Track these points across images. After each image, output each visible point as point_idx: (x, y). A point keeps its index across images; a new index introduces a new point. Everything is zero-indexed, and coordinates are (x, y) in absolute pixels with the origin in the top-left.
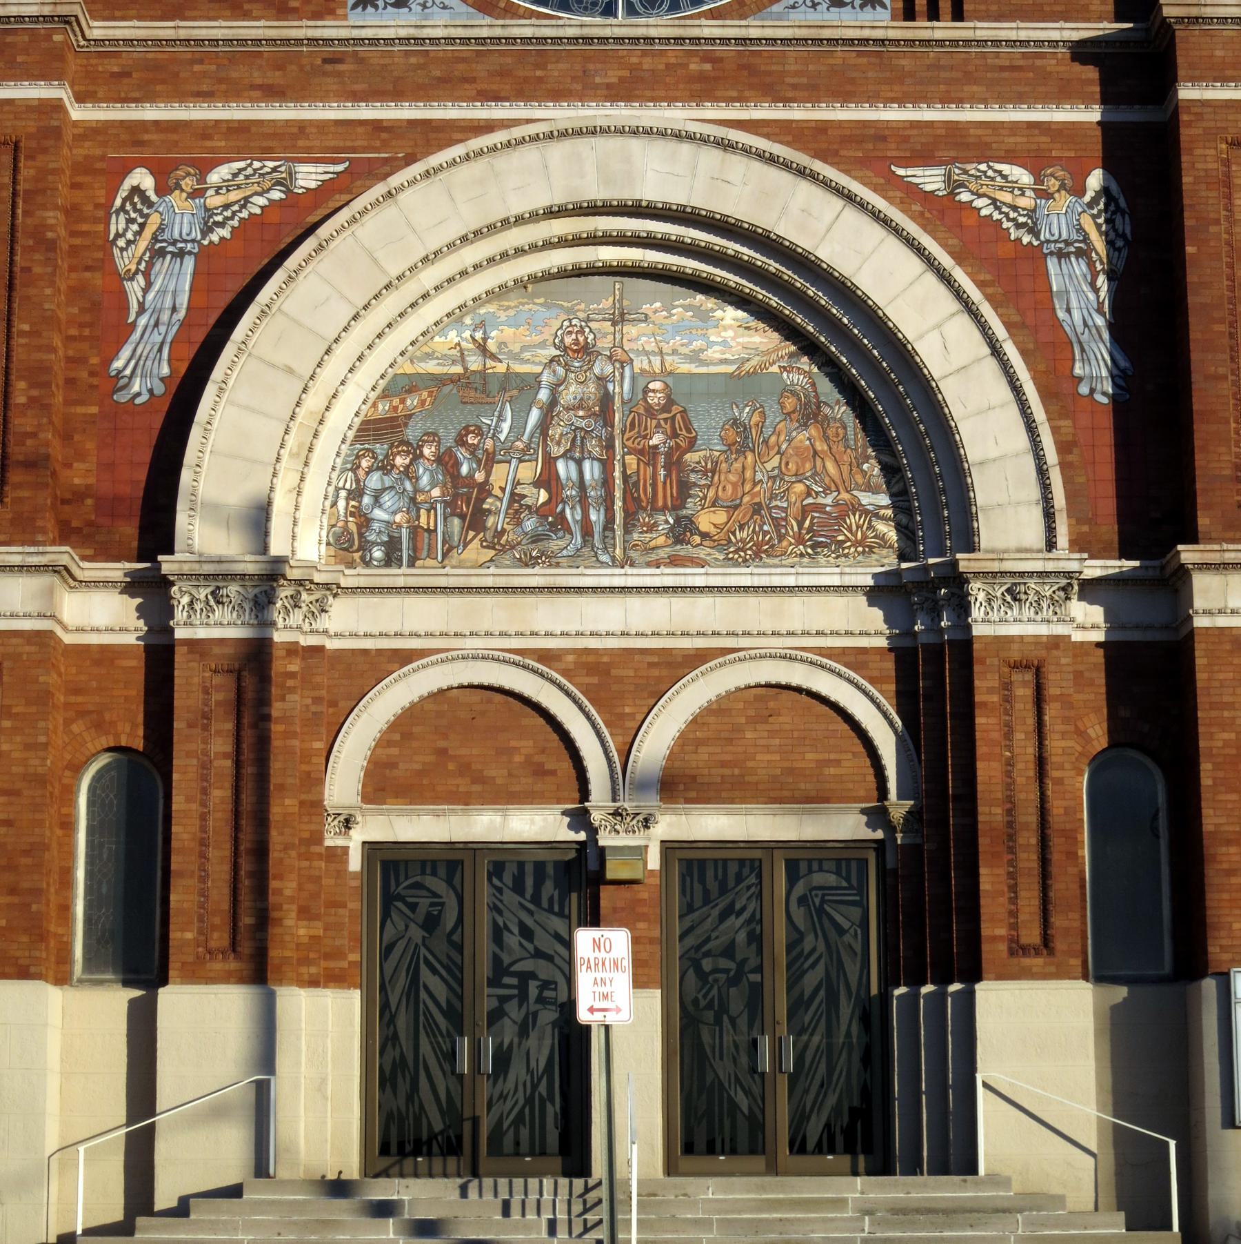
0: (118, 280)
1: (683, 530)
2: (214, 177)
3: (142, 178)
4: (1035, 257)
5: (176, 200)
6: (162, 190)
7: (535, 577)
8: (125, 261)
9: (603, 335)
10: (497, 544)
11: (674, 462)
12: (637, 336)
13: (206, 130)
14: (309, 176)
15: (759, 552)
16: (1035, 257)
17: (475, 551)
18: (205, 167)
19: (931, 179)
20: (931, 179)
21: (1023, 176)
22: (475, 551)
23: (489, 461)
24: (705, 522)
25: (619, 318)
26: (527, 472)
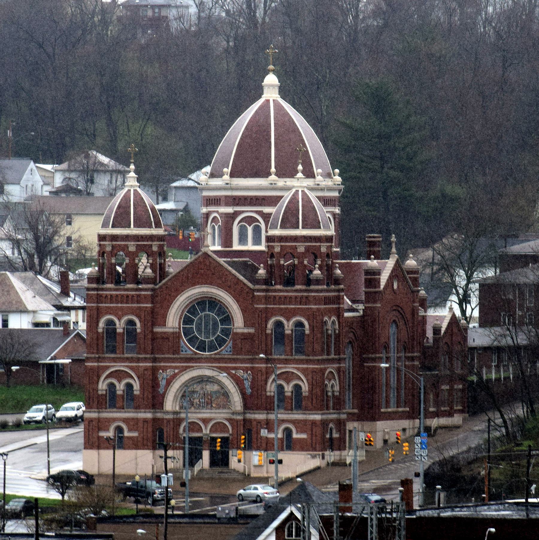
0: (159, 381)
1: (212, 406)
2: (168, 371)
3: (161, 371)
4: (243, 380)
5: (164, 374)
6: (163, 372)
7: (198, 411)
8: (160, 379)
9: (204, 387)
10: (195, 408)
11: (211, 400)
12: (207, 387)
13: (167, 366)
14: (176, 371)
15: (219, 408)
16: (243, 380)
17: (193, 408)
18: (166, 370)
19: (234, 372)
20: (234, 372)
21: (242, 371)
22: (193, 408)
23: (194, 399)
24: (214, 405)
25: (206, 385)
26: (197, 400)
